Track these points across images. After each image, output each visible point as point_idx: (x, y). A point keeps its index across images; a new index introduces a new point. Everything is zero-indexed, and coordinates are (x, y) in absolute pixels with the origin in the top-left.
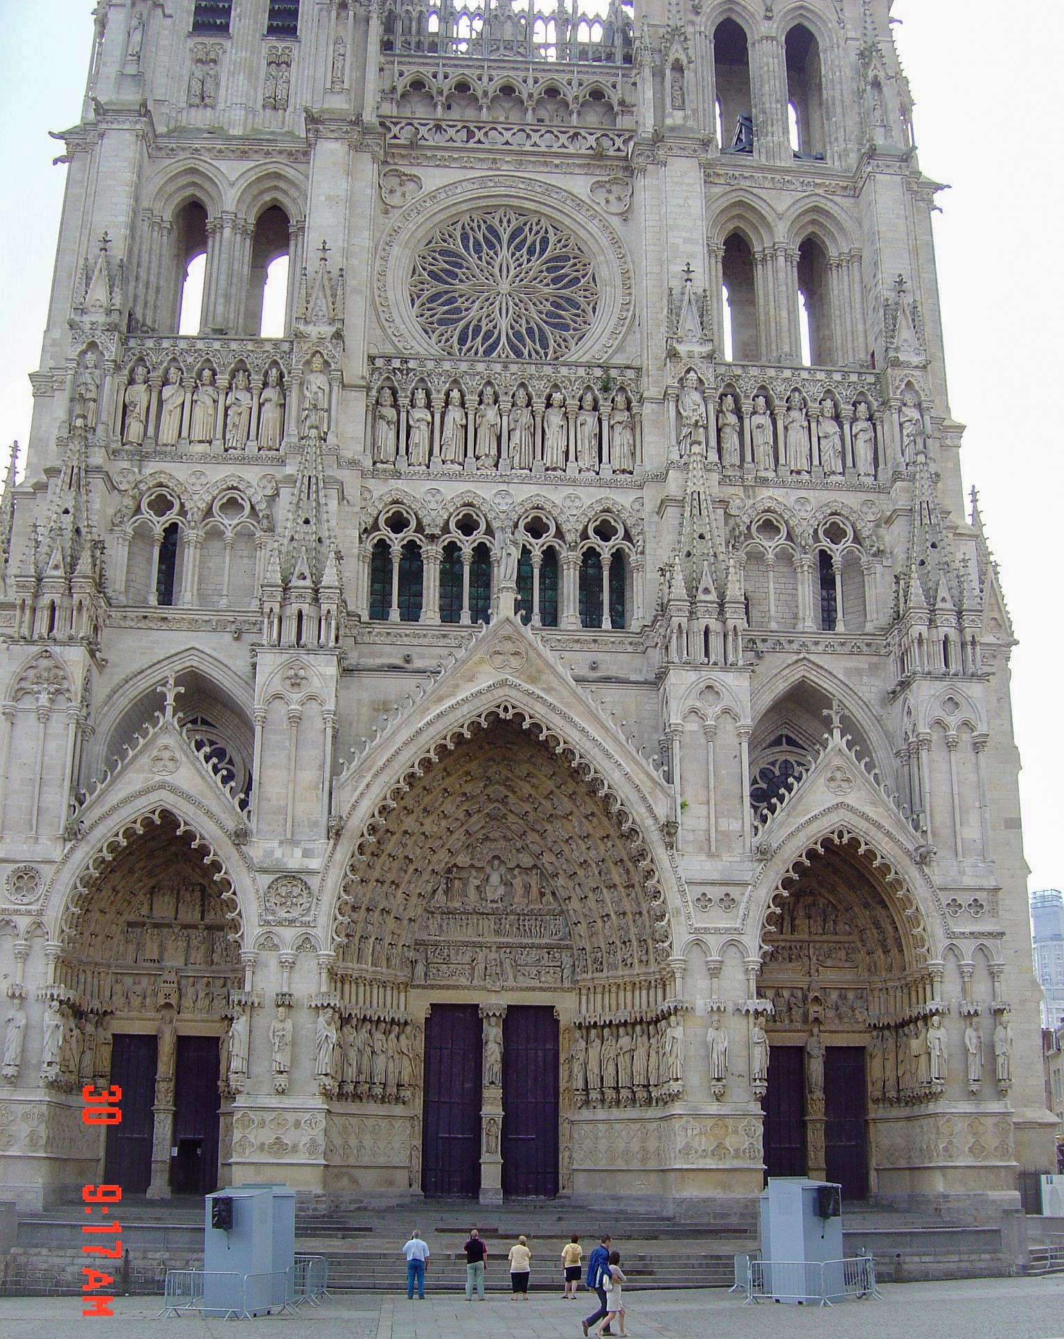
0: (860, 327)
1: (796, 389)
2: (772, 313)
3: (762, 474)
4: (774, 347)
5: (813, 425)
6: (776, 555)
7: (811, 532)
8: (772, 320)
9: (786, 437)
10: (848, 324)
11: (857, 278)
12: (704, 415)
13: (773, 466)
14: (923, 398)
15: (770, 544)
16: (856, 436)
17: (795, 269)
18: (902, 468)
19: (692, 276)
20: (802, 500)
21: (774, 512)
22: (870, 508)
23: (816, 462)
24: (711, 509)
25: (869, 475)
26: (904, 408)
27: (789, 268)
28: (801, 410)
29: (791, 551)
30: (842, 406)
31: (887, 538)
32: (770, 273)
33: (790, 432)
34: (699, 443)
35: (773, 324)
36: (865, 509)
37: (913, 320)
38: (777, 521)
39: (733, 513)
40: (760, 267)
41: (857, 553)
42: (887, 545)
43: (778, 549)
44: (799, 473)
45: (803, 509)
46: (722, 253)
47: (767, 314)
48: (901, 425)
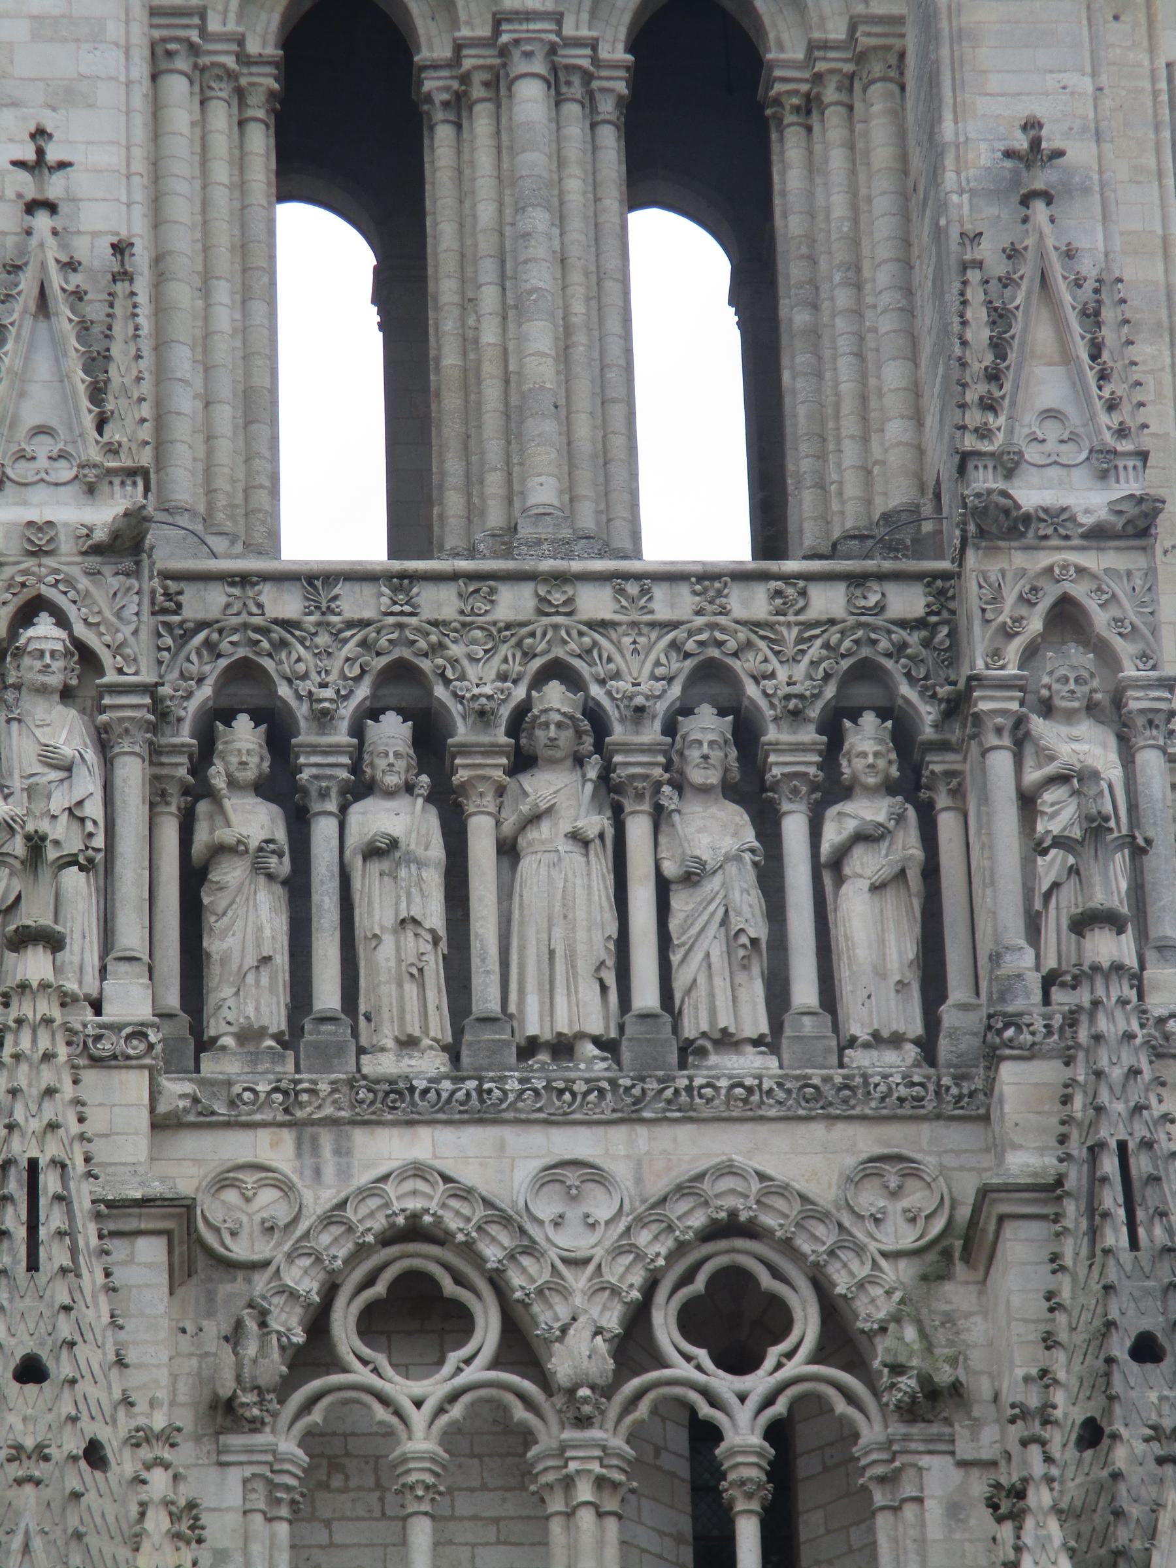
0: (893, 375)
1: (557, 671)
2: (489, 335)
3: (384, 1065)
4: (494, 483)
5: (638, 829)
6: (449, 1438)
7: (612, 1320)
8: (491, 369)
9: (506, 893)
10: (845, 366)
11: (882, 152)
12: (94, 809)
13: (439, 1026)
14: (1130, 671)
15: (418, 1388)
16: (837, 863)
17: (610, 138)
18: (1028, 1000)
19: (55, 187)
20: (572, 1177)
21: (436, 1236)
22: (895, 1194)
23: (646, 996)
24: (89, 1234)
25: (896, 1040)
26: (1038, 725)
27: (575, 131)
28: (579, 761)
29: (520, 1413)
30: (772, 734)
31: (976, 1331)
32: (484, 160)
33: (527, 864)
34: (53, 942)
35: (492, 393)
36: (870, 1199)
37: (1092, 316)
38: (460, 1280)
39: (240, 1250)
40: (444, 134)
41: (841, 1406)
42: (976, 1358)
43: (456, 1411)
44: (563, 1048)
45: (574, 1214)
46: (267, 81)
47: (469, 343)
48: (1028, 802)
